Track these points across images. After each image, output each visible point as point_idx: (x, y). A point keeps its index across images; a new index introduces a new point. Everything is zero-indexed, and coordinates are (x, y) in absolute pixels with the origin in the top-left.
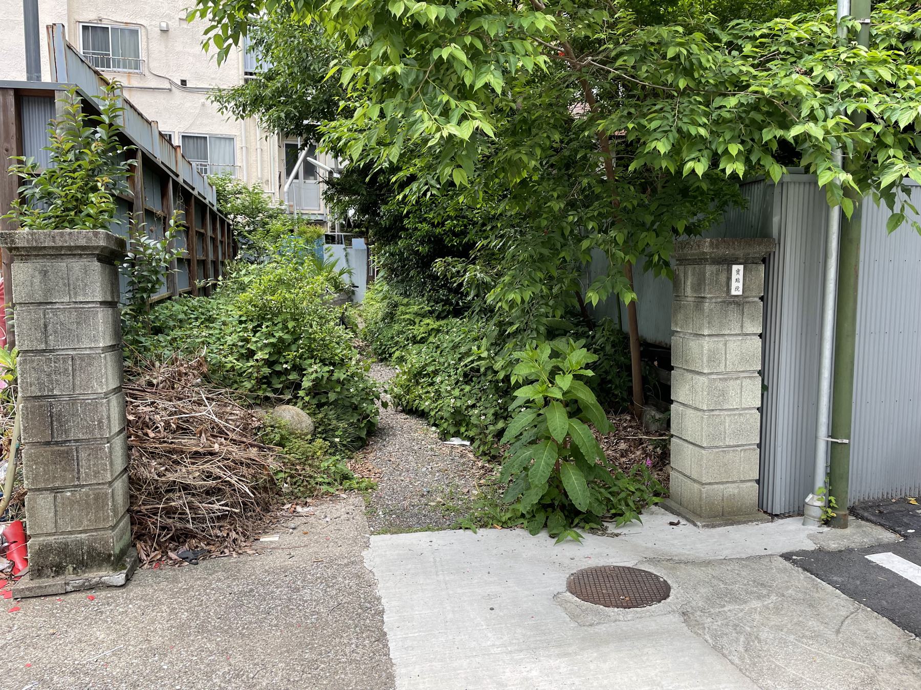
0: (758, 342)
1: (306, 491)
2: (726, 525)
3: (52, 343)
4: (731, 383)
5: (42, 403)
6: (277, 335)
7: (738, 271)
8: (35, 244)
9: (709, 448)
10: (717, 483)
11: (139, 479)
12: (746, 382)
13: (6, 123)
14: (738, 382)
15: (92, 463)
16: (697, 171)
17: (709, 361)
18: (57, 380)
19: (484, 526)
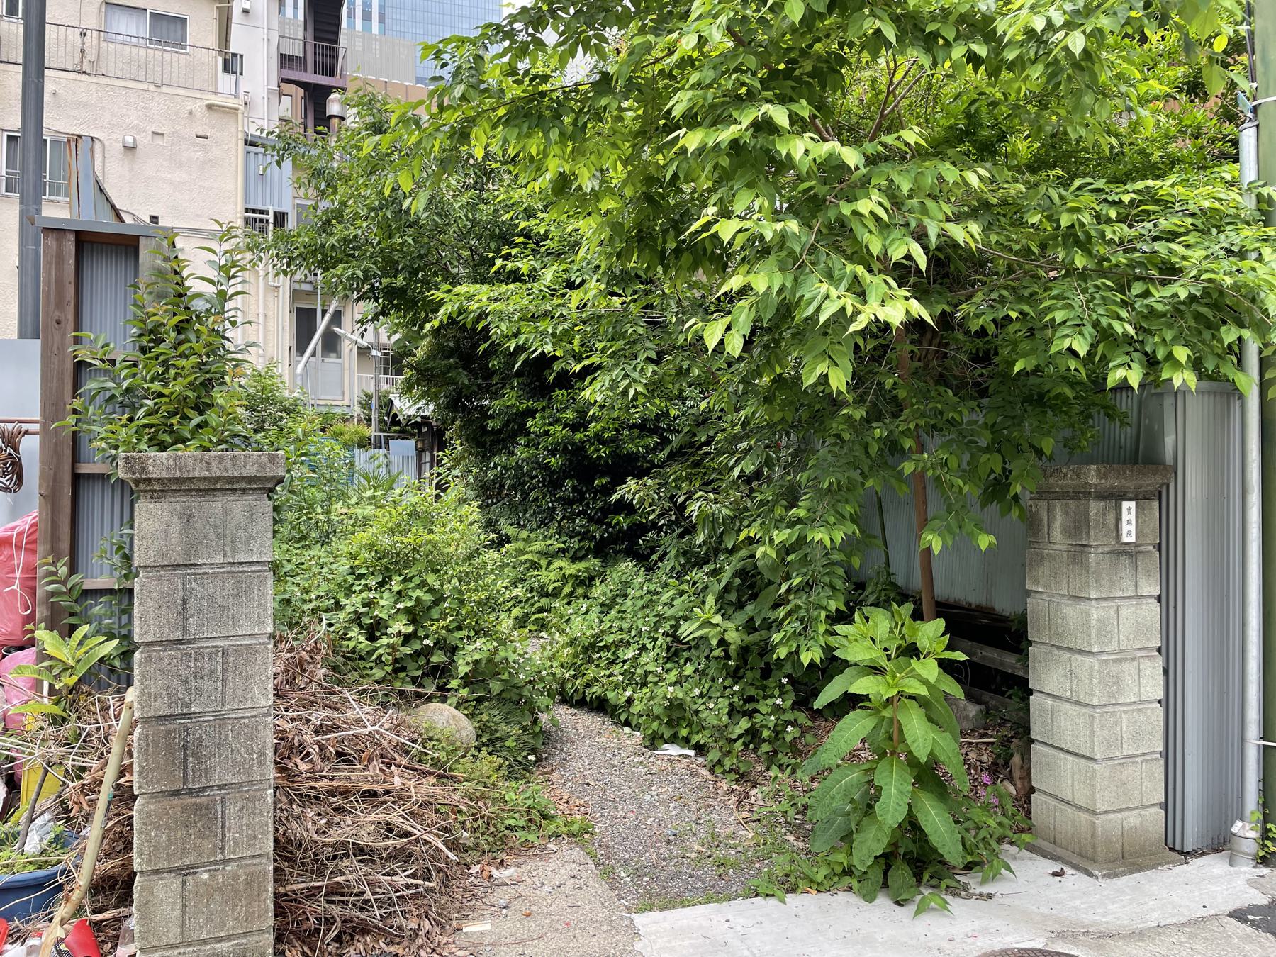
0: (1155, 607)
1: (499, 844)
2: (1131, 872)
3: (193, 629)
4: (1126, 665)
5: (171, 727)
6: (414, 595)
7: (1129, 509)
8: (178, 474)
9: (1103, 760)
10: (1114, 811)
11: (290, 842)
12: (1145, 664)
13: (59, 282)
14: (1136, 663)
15: (245, 822)
16: (1130, 382)
17: (1099, 635)
18: (197, 689)
19: (793, 889)
